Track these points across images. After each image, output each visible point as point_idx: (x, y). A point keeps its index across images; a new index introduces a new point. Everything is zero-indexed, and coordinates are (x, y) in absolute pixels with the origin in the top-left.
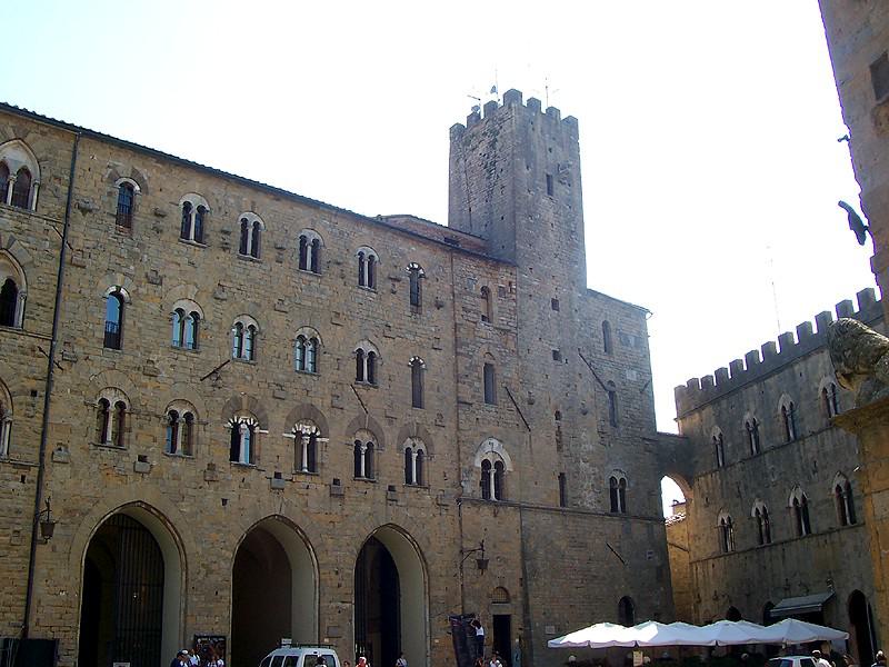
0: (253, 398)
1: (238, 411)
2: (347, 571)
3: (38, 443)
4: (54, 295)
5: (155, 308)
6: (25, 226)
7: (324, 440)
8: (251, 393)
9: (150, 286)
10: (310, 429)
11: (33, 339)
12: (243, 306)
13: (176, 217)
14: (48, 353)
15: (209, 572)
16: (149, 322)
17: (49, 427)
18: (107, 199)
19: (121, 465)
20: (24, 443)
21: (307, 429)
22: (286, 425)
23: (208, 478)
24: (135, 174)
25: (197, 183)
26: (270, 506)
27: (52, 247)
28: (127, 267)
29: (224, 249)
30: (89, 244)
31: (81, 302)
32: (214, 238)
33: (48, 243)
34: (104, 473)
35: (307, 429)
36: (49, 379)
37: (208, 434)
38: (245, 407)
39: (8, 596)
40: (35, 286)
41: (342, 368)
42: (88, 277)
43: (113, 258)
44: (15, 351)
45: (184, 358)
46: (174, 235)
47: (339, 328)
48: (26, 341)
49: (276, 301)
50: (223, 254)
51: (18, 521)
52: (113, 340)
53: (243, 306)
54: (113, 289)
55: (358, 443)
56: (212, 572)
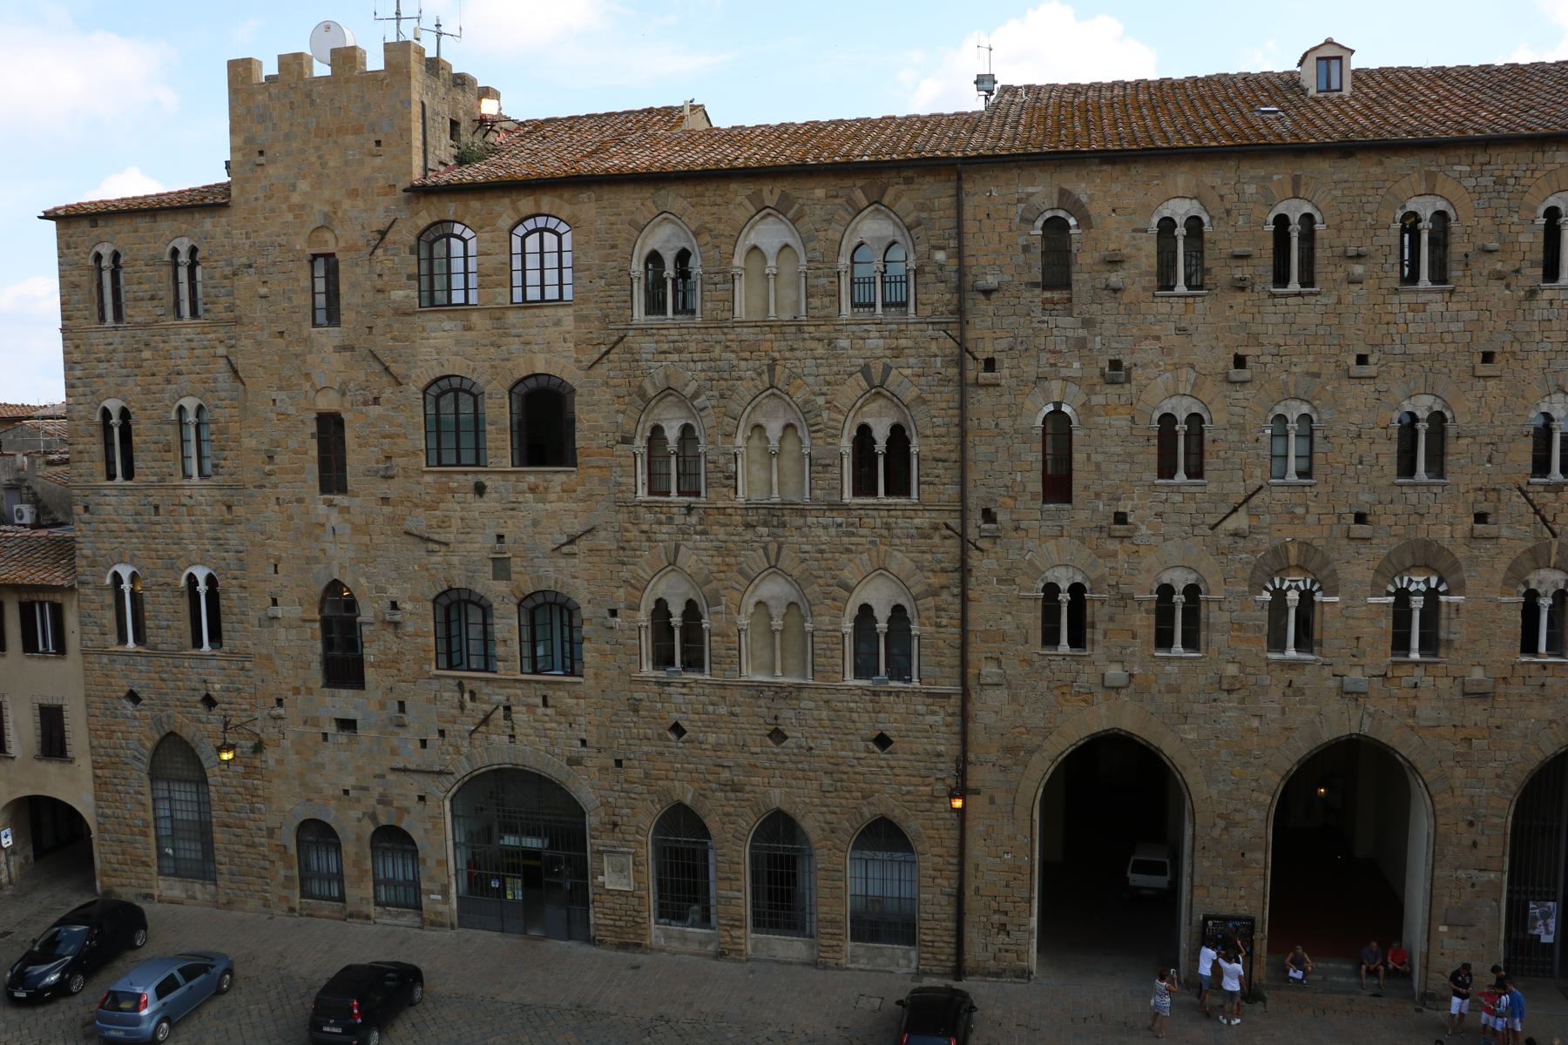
0: (1306, 546)
1: (1283, 570)
2: (1495, 820)
3: (957, 662)
4: (956, 440)
5: (1121, 422)
6: (903, 342)
7: (1454, 599)
8: (1305, 534)
9: (1110, 389)
10: (1427, 582)
11: (934, 514)
12: (1285, 383)
13: (1147, 252)
14: (959, 530)
15: (1231, 824)
16: (1118, 450)
17: (972, 637)
18: (1020, 258)
19: (1083, 678)
20: (939, 664)
21: (1417, 583)
22: (1374, 584)
23: (1225, 687)
24: (1066, 199)
25: (1182, 177)
26: (1339, 723)
27: (946, 365)
28: (1069, 365)
29: (1243, 289)
30: (1003, 344)
31: (999, 440)
32: (1221, 272)
33: (939, 359)
34: (1056, 692)
35: (1417, 583)
36: (964, 570)
37: (1225, 617)
38: (1293, 562)
39: (940, 860)
40: (928, 432)
41: (1498, 458)
42: (1006, 399)
43: (1044, 357)
44: (912, 537)
45: (1178, 498)
46: (1145, 289)
47: (1491, 383)
48: (922, 520)
49: (1352, 361)
50: (1240, 298)
51: (941, 766)
52: (1058, 486)
53: (1285, 383)
54: (1051, 408)
55: (1532, 597)
56: (1236, 824)
